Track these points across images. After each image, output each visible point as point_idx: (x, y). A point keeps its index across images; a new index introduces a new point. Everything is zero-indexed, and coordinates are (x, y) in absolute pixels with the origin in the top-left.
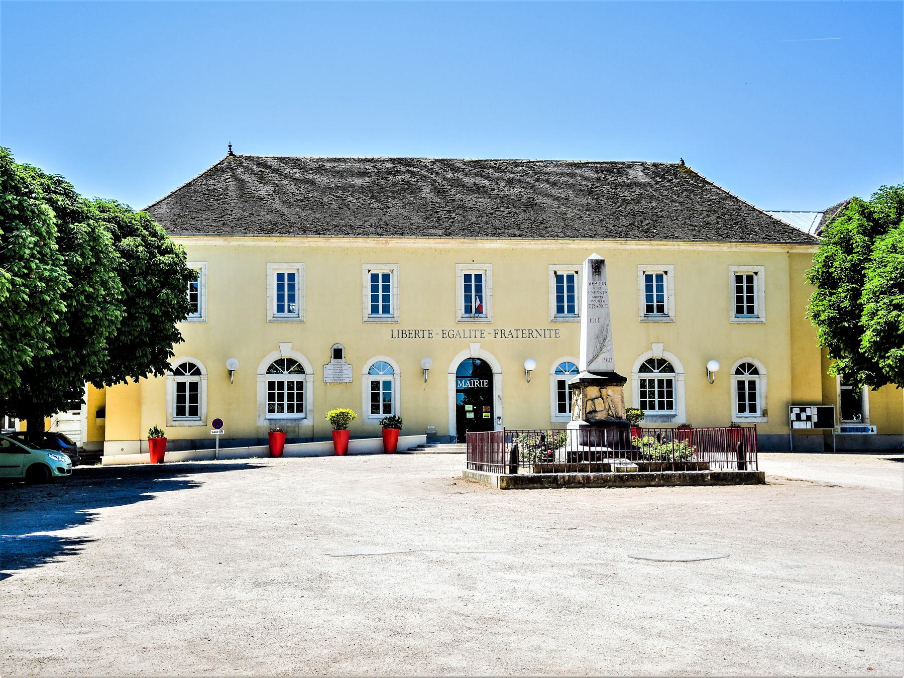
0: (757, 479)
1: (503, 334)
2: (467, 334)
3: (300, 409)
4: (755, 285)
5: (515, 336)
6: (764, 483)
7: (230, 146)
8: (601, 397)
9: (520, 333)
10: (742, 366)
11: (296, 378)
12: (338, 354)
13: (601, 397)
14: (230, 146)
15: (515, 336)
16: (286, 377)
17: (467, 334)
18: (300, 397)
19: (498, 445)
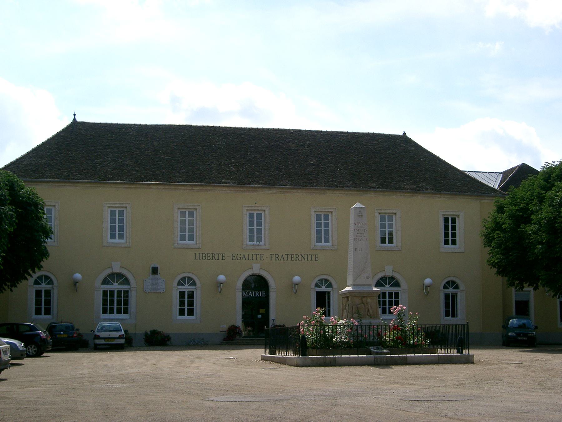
0: (469, 360)
1: (277, 258)
2: (250, 257)
3: (126, 312)
4: (457, 224)
5: (286, 259)
6: (473, 363)
7: (75, 115)
8: (363, 303)
9: (289, 257)
10: (448, 283)
11: (124, 287)
12: (155, 271)
13: (363, 303)
14: (75, 115)
15: (286, 259)
16: (116, 287)
17: (250, 257)
18: (126, 302)
19: (263, 337)
